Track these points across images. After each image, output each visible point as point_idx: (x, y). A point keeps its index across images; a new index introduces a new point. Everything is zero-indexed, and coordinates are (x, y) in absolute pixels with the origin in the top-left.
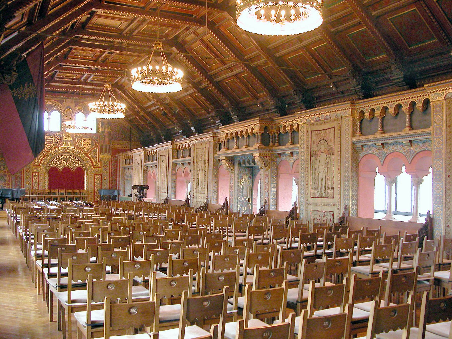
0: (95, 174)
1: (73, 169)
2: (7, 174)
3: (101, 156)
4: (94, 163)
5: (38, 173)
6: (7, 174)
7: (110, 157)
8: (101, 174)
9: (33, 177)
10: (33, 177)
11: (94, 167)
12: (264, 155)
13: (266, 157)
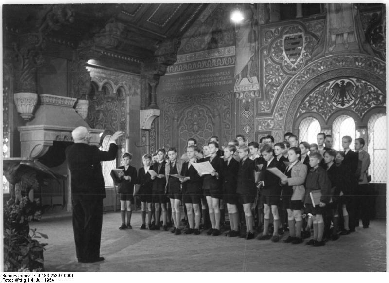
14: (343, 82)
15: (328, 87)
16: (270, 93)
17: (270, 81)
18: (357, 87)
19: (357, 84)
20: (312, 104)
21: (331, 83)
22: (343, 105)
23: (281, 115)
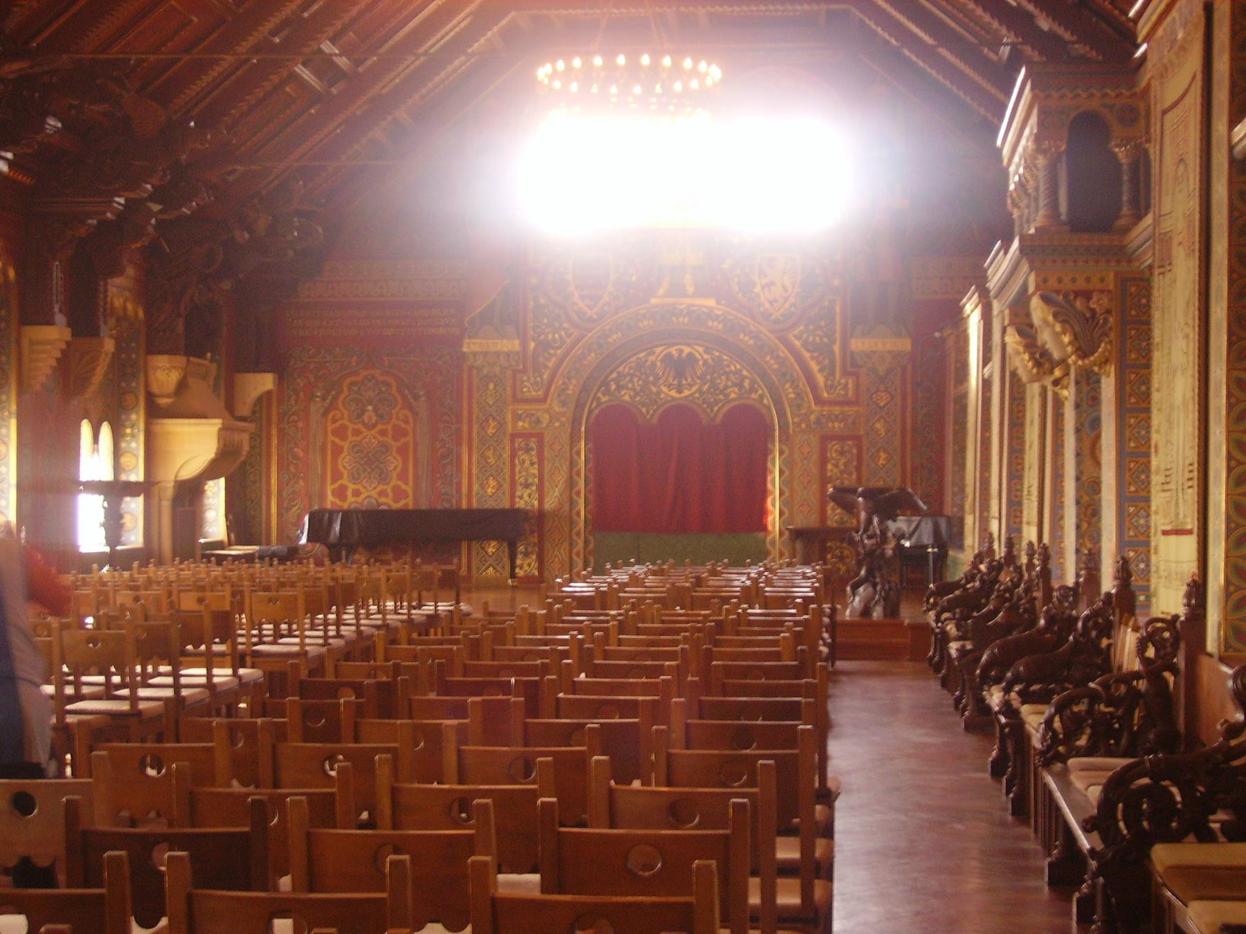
0: (825, 439)
1: (718, 412)
2: (395, 445)
3: (857, 345)
4: (820, 380)
5: (540, 437)
6: (395, 445)
7: (906, 345)
8: (857, 439)
9: (513, 456)
10: (513, 456)
11: (819, 400)
12: (1068, 285)
13: (1087, 295)
14: (681, 351)
15: (652, 358)
16: (541, 359)
17: (542, 337)
18: (705, 361)
19: (706, 357)
20: (623, 387)
21: (658, 350)
22: (680, 392)
23: (564, 404)
